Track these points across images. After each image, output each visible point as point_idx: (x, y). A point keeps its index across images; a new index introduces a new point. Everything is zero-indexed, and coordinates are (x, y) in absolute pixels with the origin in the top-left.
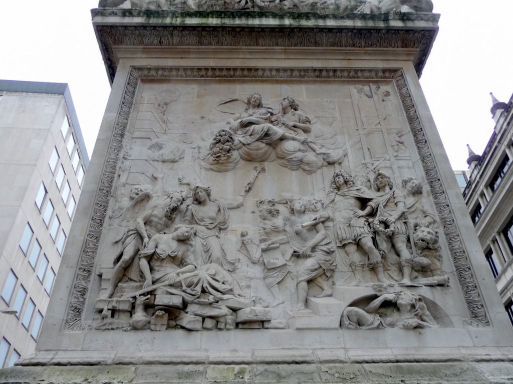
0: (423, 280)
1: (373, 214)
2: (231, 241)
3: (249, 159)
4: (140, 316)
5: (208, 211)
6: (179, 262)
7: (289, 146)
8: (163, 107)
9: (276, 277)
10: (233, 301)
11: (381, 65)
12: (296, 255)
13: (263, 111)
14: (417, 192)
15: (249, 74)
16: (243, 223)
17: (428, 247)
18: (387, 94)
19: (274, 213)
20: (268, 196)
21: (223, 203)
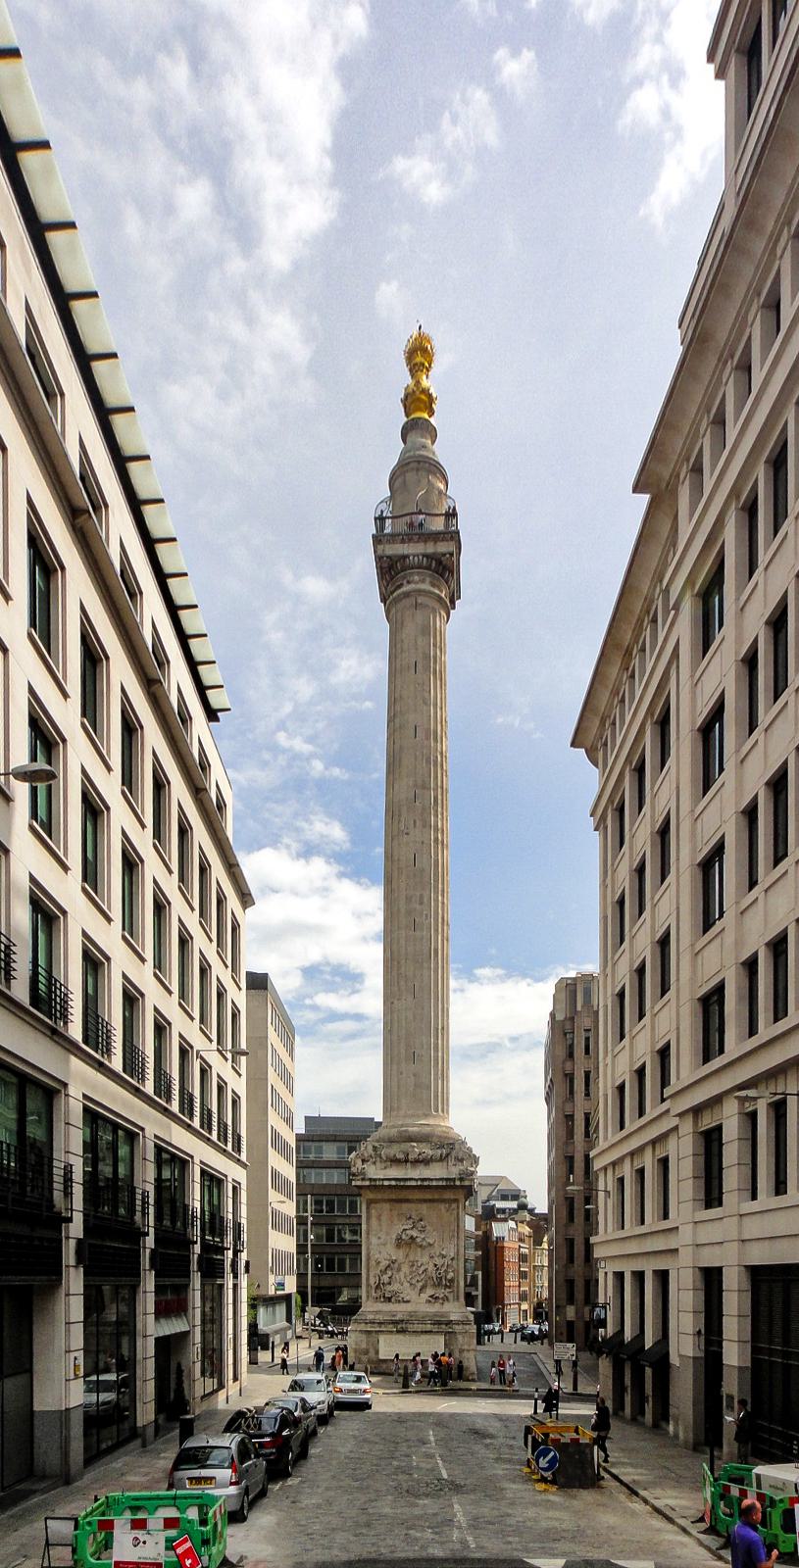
0: (448, 1290)
1: (438, 1269)
2: (402, 1274)
3: (406, 1244)
4: (382, 1300)
5: (396, 1265)
6: (390, 1284)
7: (418, 1240)
8: (379, 1218)
9: (412, 1287)
10: (402, 1295)
11: (452, 1197)
12: (418, 1281)
13: (411, 1221)
14: (452, 1259)
15: (407, 1201)
16: (405, 1269)
17: (451, 1281)
18: (453, 1209)
19: (413, 1266)
20: (412, 1259)
21: (399, 1261)
